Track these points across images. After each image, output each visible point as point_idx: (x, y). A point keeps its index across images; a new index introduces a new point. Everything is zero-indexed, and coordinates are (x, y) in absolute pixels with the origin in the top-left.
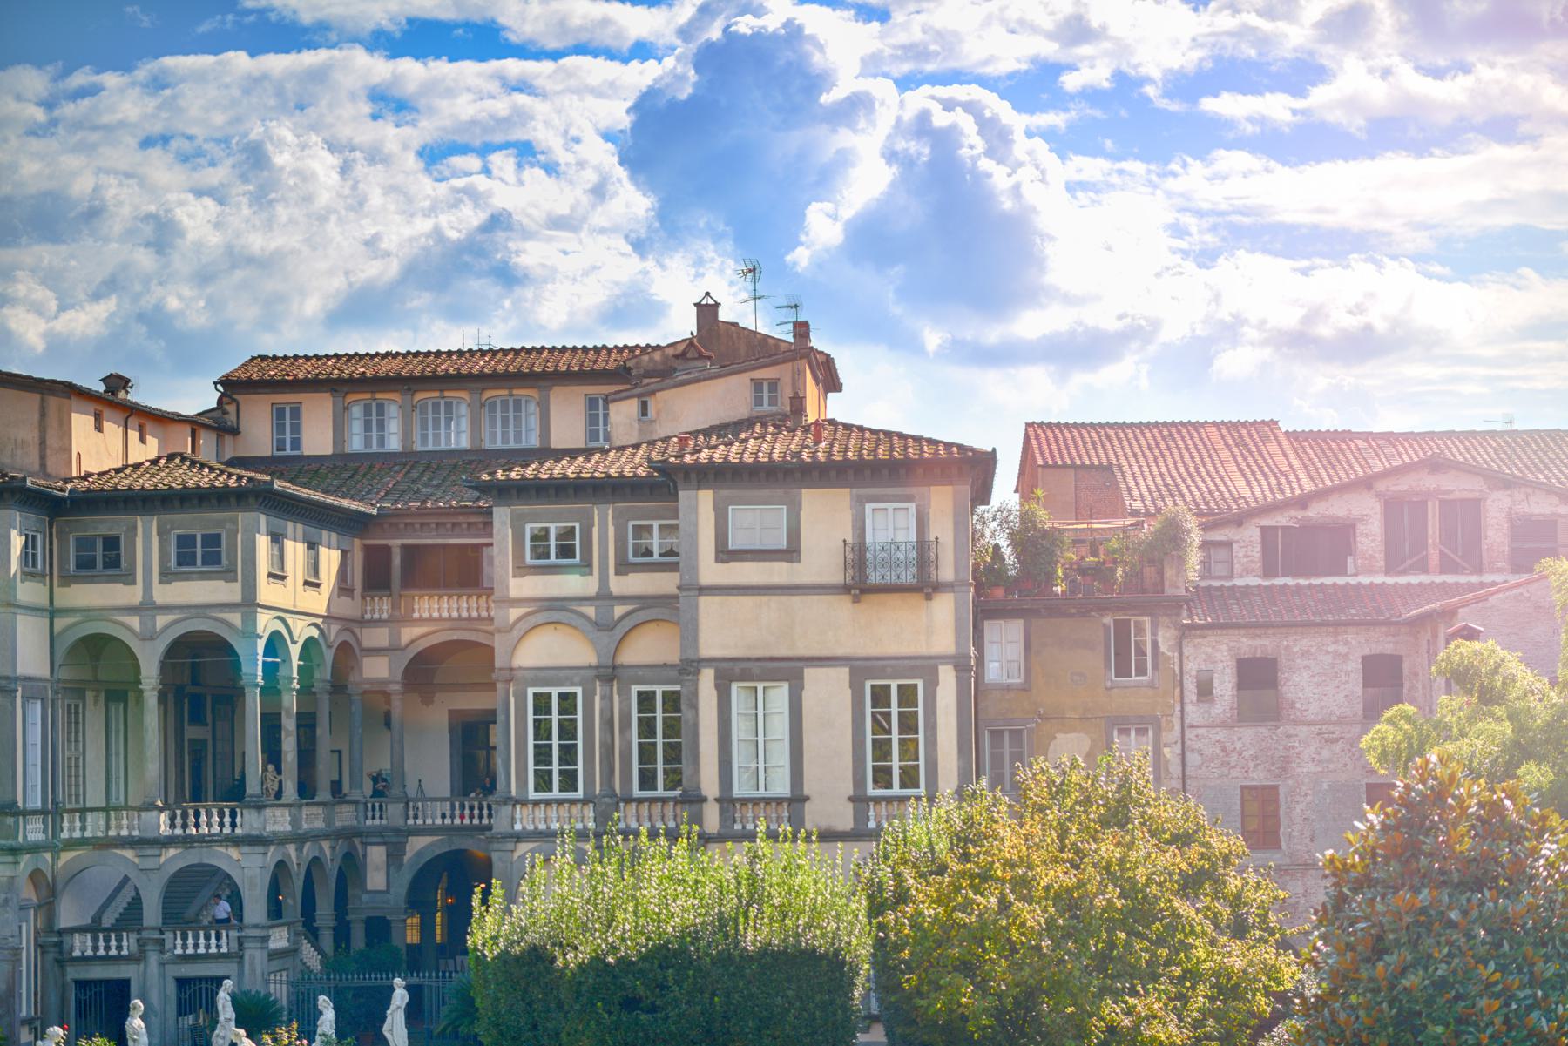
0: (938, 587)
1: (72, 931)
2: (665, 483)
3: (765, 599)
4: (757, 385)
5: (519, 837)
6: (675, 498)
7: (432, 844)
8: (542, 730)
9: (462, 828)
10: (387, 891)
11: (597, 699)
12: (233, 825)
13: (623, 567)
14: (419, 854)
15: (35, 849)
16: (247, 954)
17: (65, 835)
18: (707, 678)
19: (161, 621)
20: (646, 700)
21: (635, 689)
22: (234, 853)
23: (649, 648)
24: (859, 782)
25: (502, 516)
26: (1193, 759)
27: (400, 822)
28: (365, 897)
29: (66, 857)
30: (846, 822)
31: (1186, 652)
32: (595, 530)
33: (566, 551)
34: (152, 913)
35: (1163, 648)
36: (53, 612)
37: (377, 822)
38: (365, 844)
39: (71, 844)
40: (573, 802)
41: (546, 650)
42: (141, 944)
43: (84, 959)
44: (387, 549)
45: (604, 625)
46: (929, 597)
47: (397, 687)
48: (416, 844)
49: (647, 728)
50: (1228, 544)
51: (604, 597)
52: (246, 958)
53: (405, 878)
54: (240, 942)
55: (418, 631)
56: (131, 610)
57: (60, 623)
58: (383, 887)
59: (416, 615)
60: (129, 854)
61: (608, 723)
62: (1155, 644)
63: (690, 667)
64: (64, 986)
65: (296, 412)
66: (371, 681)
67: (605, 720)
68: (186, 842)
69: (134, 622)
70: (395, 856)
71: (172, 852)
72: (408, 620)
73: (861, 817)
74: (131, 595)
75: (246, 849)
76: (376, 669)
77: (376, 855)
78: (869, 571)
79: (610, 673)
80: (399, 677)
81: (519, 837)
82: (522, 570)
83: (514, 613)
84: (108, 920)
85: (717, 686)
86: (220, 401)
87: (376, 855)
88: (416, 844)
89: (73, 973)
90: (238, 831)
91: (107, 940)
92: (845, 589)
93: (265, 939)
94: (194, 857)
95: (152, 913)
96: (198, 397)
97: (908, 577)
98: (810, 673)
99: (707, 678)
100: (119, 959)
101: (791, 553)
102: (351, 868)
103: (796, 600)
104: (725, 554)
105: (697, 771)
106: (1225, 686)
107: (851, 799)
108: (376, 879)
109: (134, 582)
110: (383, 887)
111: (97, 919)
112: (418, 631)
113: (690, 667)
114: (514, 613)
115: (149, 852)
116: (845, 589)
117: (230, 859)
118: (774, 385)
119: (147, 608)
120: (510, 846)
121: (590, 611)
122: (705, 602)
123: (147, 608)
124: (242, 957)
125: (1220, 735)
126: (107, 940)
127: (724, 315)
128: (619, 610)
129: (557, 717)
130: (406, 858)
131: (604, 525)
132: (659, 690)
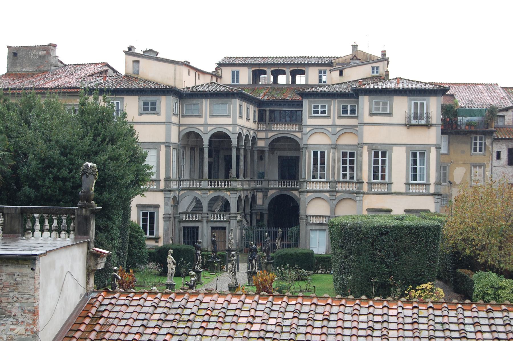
0: (431, 125)
1: (183, 213)
2: (356, 93)
4: (373, 68)
5: (308, 191)
6: (358, 99)
7: (275, 193)
8: (315, 162)
10: (263, 205)
11: (331, 153)
12: (228, 185)
13: (340, 117)
14: (272, 195)
15: (174, 190)
16: (231, 221)
17: (181, 187)
18: (366, 148)
19: (210, 128)
20: (345, 154)
22: (228, 193)
23: (347, 140)
24: (407, 179)
25: (306, 103)
26: (494, 175)
27: (267, 187)
28: (256, 206)
29: (182, 193)
30: (403, 190)
31: (494, 145)
32: (332, 106)
33: (323, 112)
34: (205, 209)
35: (487, 144)
36: (180, 125)
37: (260, 186)
38: (257, 192)
39: (183, 189)
40: (323, 182)
41: (317, 141)
42: (202, 217)
43: (186, 221)
44: (265, 111)
46: (429, 128)
47: (267, 149)
48: (271, 192)
49: (344, 162)
50: (504, 116)
51: (334, 126)
52: (231, 222)
53: (267, 202)
54: (229, 217)
57: (182, 128)
58: (262, 204)
59: (273, 129)
60: (199, 192)
61: (334, 160)
62: (485, 143)
63: (360, 146)
64: (180, 228)
65: (238, 72)
67: (333, 159)
68: (215, 190)
69: (202, 128)
70: (265, 196)
71: (211, 192)
73: (408, 189)
74: (201, 121)
75: (232, 192)
76: (261, 144)
77: (260, 195)
78: (412, 120)
79: (335, 147)
80: (267, 146)
81: (308, 191)
82: (311, 117)
83: (309, 129)
84: (189, 211)
85: (368, 151)
86: (216, 69)
87: (260, 195)
89: (183, 225)
90: (229, 187)
91: (189, 216)
92: (406, 125)
93: (236, 217)
94: (217, 194)
95: (205, 209)
96: (211, 68)
97: (423, 122)
98: (395, 148)
99: (366, 148)
100: (196, 221)
101: (390, 114)
102: (254, 198)
103: (391, 128)
104: (372, 114)
105: (362, 174)
106: (504, 155)
107: (405, 184)
108: (259, 202)
109: (202, 117)
110: (262, 204)
111: (187, 210)
113: (360, 146)
114: (309, 129)
115: (204, 192)
116: (406, 125)
117: (227, 195)
118: (377, 68)
120: (306, 194)
121: (330, 129)
122: (366, 128)
123: (206, 125)
124: (230, 222)
125: (503, 169)
126: (189, 216)
127: (359, 48)
128: (338, 129)
129: (319, 158)
131: (335, 106)
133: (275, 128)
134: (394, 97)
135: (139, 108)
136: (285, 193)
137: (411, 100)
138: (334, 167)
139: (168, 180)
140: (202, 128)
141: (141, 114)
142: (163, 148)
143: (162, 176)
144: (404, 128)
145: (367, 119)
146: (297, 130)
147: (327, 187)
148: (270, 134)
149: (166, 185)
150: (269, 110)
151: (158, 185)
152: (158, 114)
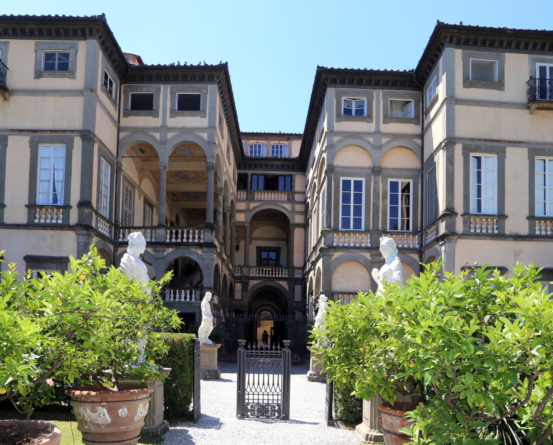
3: (487, 109)
7: (258, 283)
9: (269, 278)
14: (254, 286)
19: (170, 135)
21: (389, 180)
37: (239, 275)
45: (379, 147)
49: (394, 200)
55: (256, 204)
56: (156, 129)
58: (240, 299)
66: (239, 222)
69: (157, 135)
72: (253, 200)
76: (240, 218)
80: (249, 221)
88: (253, 283)
101: (500, 85)
103: (502, 111)
104: (467, 83)
110: (240, 299)
112: (256, 204)
119: (164, 128)
130: (249, 288)
132: (400, 181)
133: (259, 196)
134: (506, 54)
135: (37, 63)
136: (271, 284)
137: (534, 61)
138: (376, 206)
139: (84, 204)
140: (157, 135)
141: (38, 75)
142: (78, 142)
143: (75, 198)
144: (526, 112)
145: (461, 92)
146: (286, 200)
147: (366, 241)
148: (252, 205)
149: (80, 215)
150: (252, 175)
151: (66, 216)
152: (73, 76)
